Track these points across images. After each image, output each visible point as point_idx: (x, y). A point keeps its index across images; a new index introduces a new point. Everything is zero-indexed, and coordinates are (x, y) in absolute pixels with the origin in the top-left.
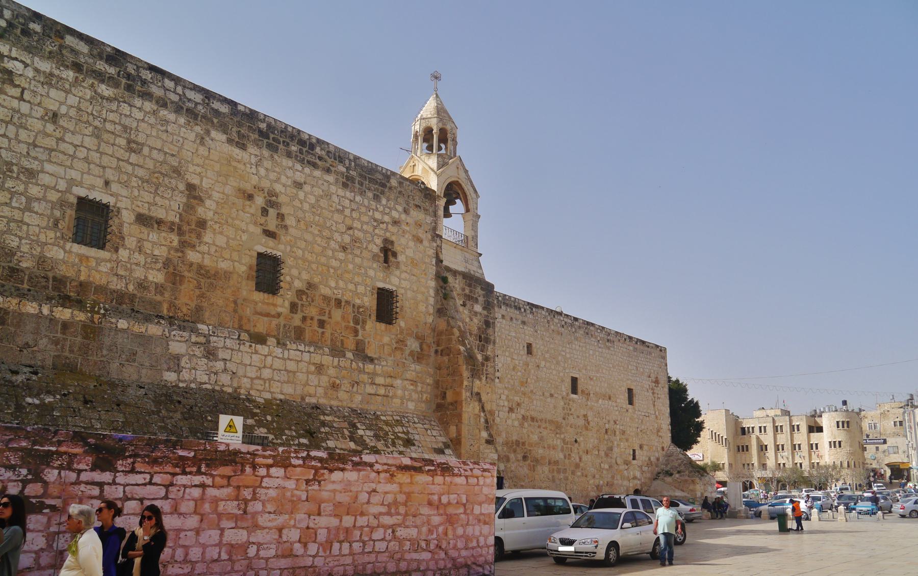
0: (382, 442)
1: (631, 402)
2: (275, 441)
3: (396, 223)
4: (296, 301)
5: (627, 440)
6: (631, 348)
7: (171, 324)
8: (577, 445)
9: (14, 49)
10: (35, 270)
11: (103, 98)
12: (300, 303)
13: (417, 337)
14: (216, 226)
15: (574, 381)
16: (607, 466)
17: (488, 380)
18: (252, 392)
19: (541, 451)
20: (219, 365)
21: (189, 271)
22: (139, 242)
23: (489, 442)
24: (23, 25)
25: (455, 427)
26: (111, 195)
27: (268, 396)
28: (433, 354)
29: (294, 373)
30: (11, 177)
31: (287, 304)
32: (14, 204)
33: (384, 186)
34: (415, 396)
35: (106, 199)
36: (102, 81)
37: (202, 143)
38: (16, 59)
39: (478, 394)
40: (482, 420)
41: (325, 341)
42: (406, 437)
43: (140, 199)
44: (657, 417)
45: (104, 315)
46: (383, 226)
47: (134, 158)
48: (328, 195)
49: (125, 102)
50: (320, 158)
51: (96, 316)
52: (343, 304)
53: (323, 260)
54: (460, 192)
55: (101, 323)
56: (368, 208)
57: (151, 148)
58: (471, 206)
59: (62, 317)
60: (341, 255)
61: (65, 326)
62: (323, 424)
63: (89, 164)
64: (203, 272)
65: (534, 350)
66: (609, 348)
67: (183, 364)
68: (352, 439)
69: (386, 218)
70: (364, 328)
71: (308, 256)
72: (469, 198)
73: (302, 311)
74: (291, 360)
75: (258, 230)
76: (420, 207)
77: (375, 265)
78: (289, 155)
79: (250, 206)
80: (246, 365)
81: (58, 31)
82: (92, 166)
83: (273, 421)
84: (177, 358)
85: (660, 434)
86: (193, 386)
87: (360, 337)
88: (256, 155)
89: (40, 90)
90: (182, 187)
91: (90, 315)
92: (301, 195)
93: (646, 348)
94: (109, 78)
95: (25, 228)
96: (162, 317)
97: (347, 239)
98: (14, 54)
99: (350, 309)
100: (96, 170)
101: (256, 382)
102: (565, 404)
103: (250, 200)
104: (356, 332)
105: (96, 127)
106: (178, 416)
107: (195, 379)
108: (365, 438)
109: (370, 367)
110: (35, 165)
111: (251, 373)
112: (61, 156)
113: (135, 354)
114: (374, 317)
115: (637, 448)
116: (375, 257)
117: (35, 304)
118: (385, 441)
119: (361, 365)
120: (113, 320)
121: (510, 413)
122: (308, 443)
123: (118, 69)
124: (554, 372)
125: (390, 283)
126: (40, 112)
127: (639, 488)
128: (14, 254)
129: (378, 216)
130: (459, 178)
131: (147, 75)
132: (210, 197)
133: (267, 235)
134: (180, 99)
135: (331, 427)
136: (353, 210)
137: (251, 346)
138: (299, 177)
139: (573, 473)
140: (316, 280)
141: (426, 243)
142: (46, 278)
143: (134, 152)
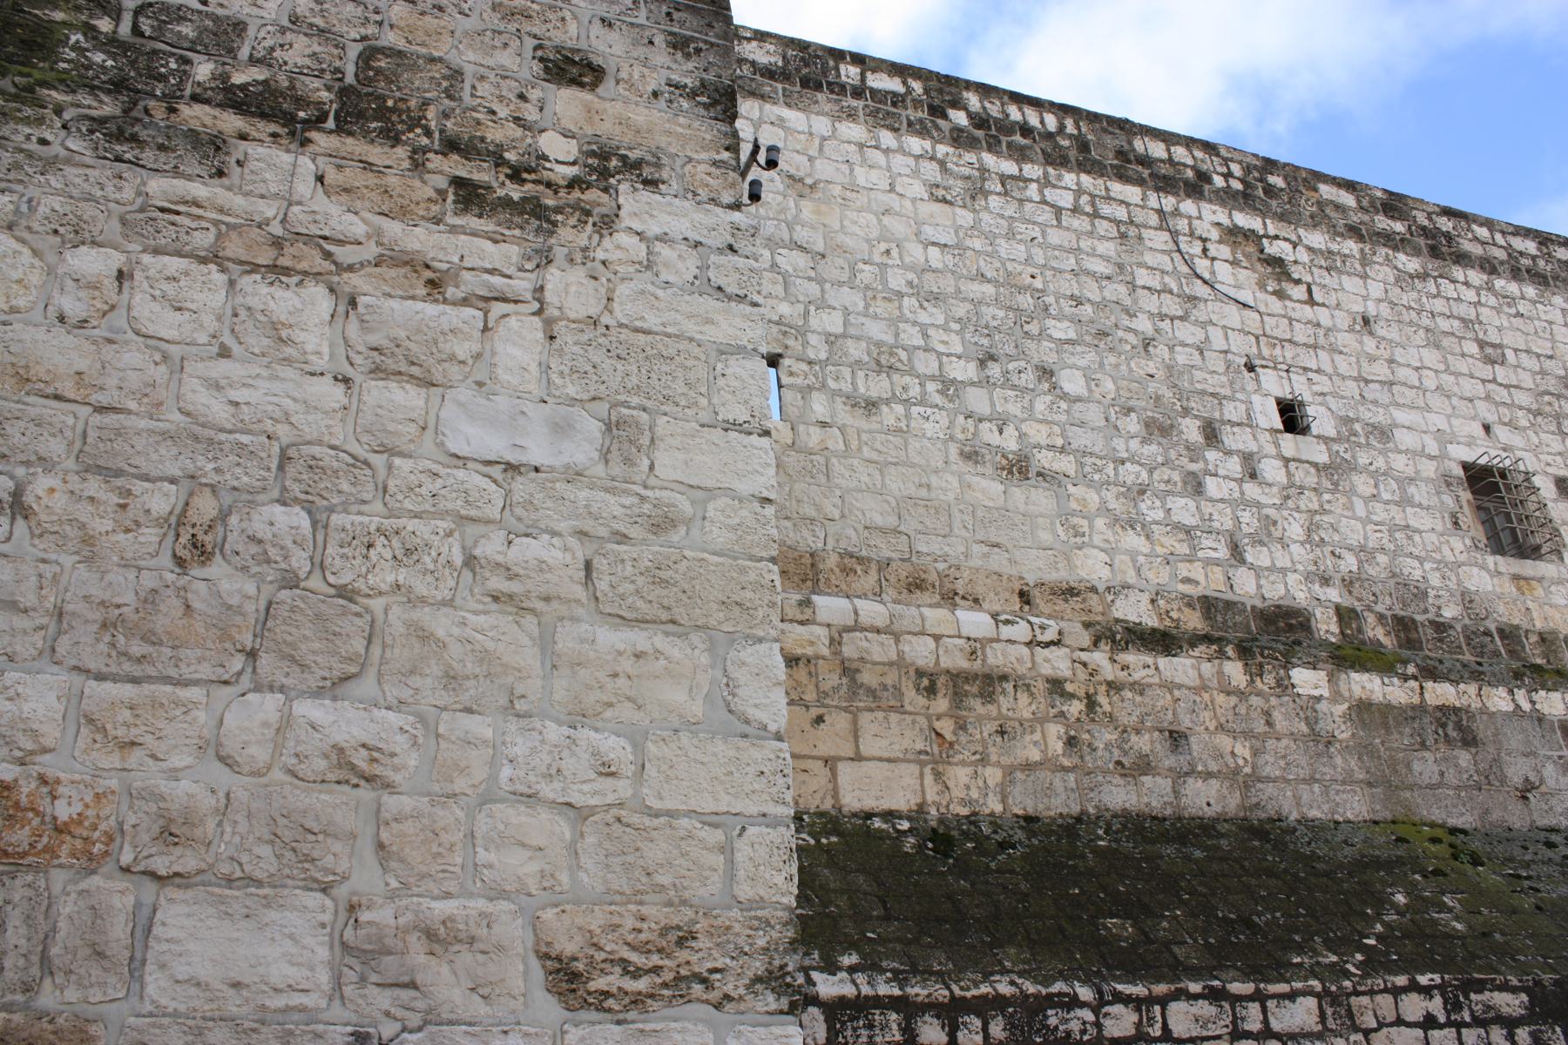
9: (1268, 221)
10: (1467, 621)
24: (1261, 180)
30: (1359, 445)
32: (1386, 496)
36: (1395, 248)
38: (1276, 237)
43: (1546, 449)
47: (1501, 373)
63: (1448, 397)
81: (1305, 180)
89: (1327, 280)
94: (1402, 240)
95: (1417, 538)
98: (1272, 231)
100: (1464, 408)
110: (1380, 417)
112: (1407, 391)
126: (1343, 320)
128: (1425, 594)
131: (1446, 224)
142: (1487, 633)
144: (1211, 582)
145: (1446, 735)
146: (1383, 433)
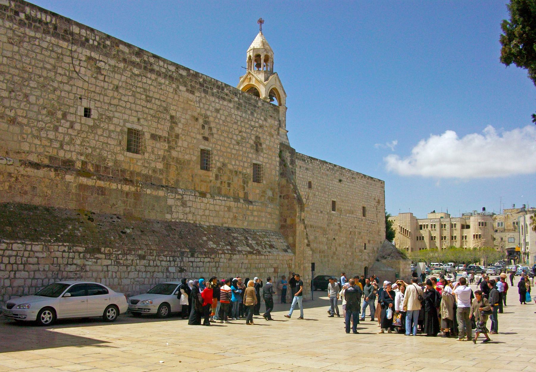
0: (260, 247)
1: (364, 215)
2: (217, 248)
3: (261, 127)
4: (218, 173)
5: (362, 238)
6: (365, 182)
7: (167, 190)
8: (334, 241)
9: (101, 56)
10: (114, 167)
11: (136, 75)
12: (219, 174)
13: (271, 189)
14: (183, 137)
15: (334, 203)
16: (350, 254)
18: (202, 223)
19: (315, 245)
20: (188, 210)
21: (173, 162)
22: (152, 148)
23: (308, 245)
24: (103, 42)
25: (292, 238)
26: (141, 125)
27: (208, 224)
28: (278, 198)
30: (102, 121)
31: (214, 176)
32: (105, 135)
33: (255, 106)
34: (271, 221)
35: (140, 128)
36: (134, 67)
37: (176, 94)
38: (101, 61)
39: (303, 220)
40: (305, 234)
42: (269, 243)
44: (378, 223)
45: (141, 187)
46: (255, 129)
48: (230, 115)
49: (144, 76)
50: (227, 95)
51: (139, 188)
52: (238, 173)
53: (229, 150)
54: (276, 93)
56: (249, 120)
57: (156, 99)
58: (282, 102)
60: (237, 147)
61: (127, 194)
62: (234, 238)
64: (178, 161)
65: (313, 185)
66: (352, 182)
67: (173, 210)
68: (248, 246)
69: (257, 125)
71: (222, 148)
72: (281, 97)
73: (220, 179)
75: (200, 137)
77: (252, 151)
78: (213, 95)
79: (197, 125)
80: (198, 209)
81: (116, 43)
82: (133, 111)
83: (214, 238)
84: (171, 207)
85: (380, 234)
86: (178, 221)
87: (246, 191)
88: (199, 97)
89: (111, 75)
90: (168, 117)
92: (219, 116)
93: (373, 182)
94: (138, 64)
95: (109, 146)
96: (163, 186)
97: (239, 138)
98: (101, 59)
99: (241, 176)
100: (134, 114)
101: (203, 217)
103: (196, 121)
104: (244, 188)
105: (133, 91)
106: (177, 236)
107: (178, 217)
108: (253, 245)
109: (251, 207)
110: (111, 115)
111: (201, 212)
113: (154, 206)
114: (252, 180)
115: (367, 242)
116: (252, 146)
117: (115, 184)
118: (261, 246)
119: (247, 206)
120: (145, 190)
123: (140, 59)
124: (323, 198)
126: (111, 87)
127: (367, 266)
128: (106, 160)
129: (253, 123)
131: (152, 60)
132: (180, 122)
133: (205, 140)
134: (166, 71)
135: (238, 239)
136: (242, 122)
138: (218, 106)
139: (332, 257)
140: (226, 161)
141: (275, 137)
142: (118, 170)
143: (149, 102)
144: (52, 152)
145: (98, 192)
146: (110, 119)
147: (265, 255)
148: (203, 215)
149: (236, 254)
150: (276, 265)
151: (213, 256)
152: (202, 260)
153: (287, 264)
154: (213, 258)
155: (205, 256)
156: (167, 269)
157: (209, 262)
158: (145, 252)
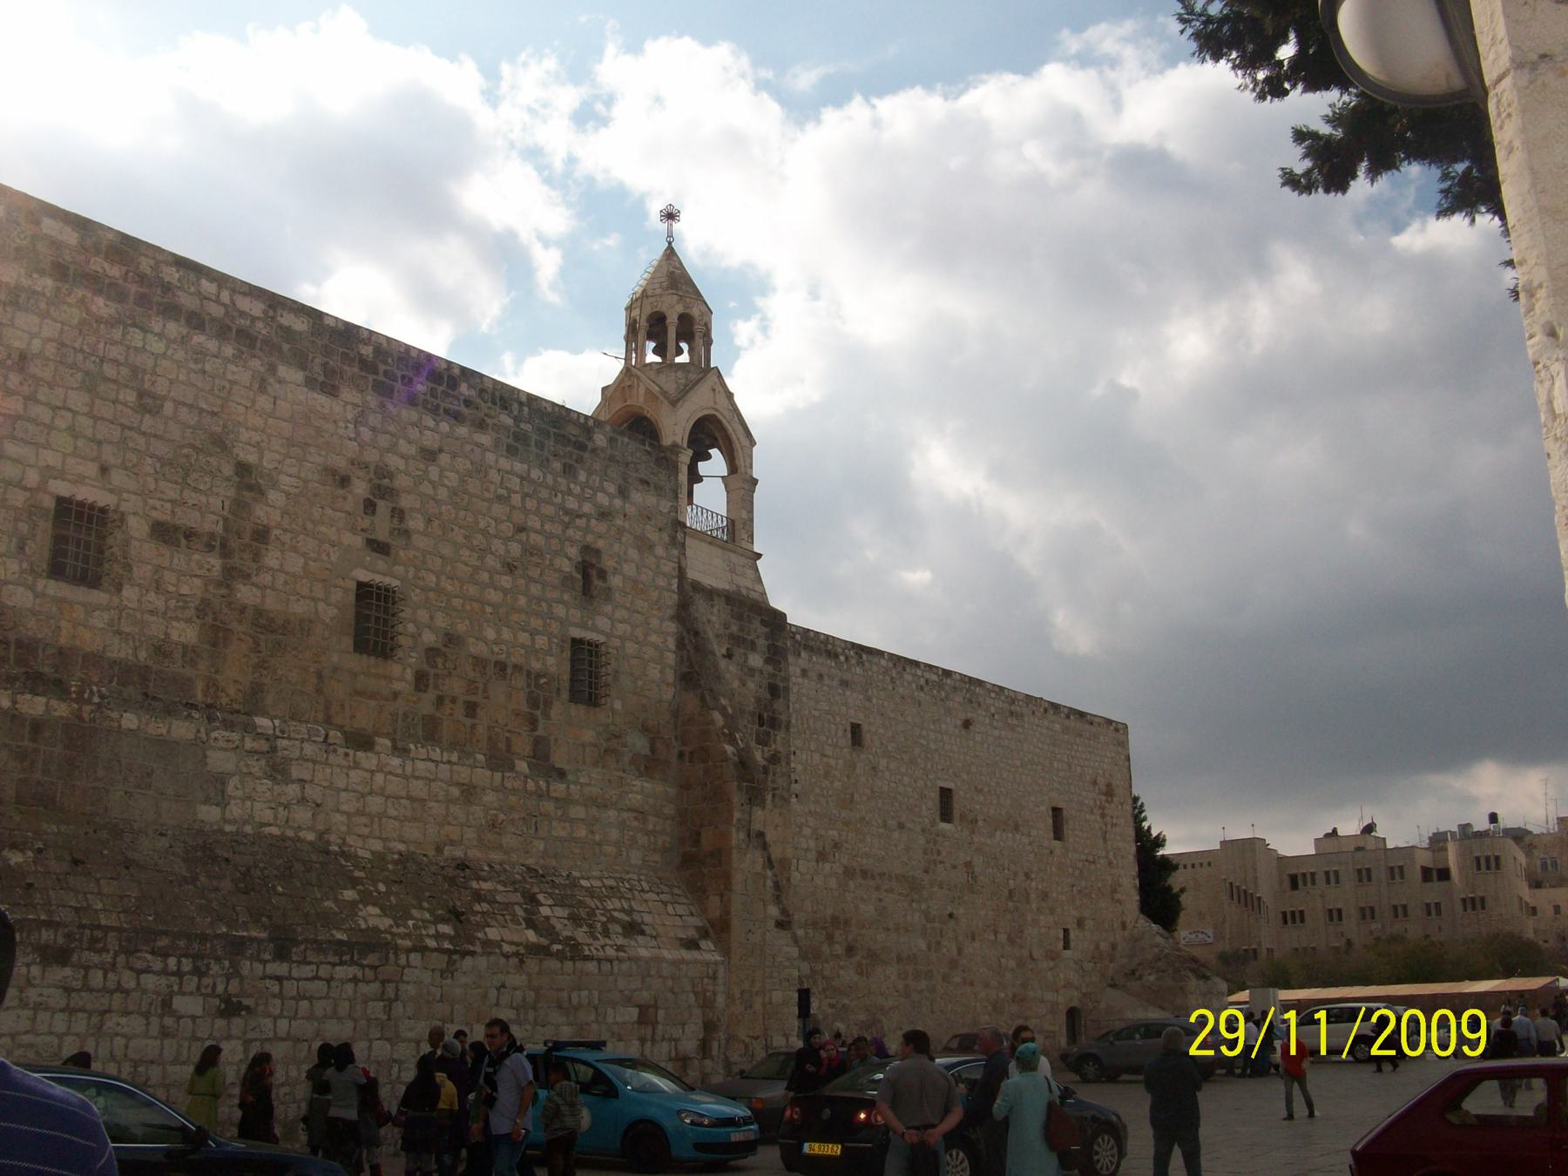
0: (585, 929)
1: (1058, 834)
2: (395, 930)
3: (604, 514)
4: (426, 667)
5: (1052, 911)
6: (1057, 727)
7: (210, 719)
8: (952, 923)
11: (99, 320)
12: (432, 671)
13: (645, 729)
14: (287, 537)
15: (946, 795)
16: (1012, 964)
17: (776, 800)
18: (350, 840)
20: (293, 790)
21: (240, 622)
22: (156, 572)
23: (782, 925)
25: (717, 899)
26: (111, 491)
27: (377, 846)
28: (674, 759)
29: (423, 801)
31: (409, 675)
33: (581, 447)
34: (642, 840)
35: (102, 498)
36: (99, 292)
37: (263, 389)
39: (761, 835)
40: (769, 883)
41: (478, 741)
42: (627, 918)
43: (159, 495)
44: (1110, 863)
45: (99, 706)
46: (581, 522)
47: (148, 420)
48: (480, 470)
49: (135, 325)
50: (468, 403)
51: (87, 708)
52: (509, 671)
53: (472, 590)
55: (95, 721)
56: (554, 490)
57: (178, 404)
58: (740, 462)
59: (31, 712)
60: (506, 581)
61: (37, 727)
62: (478, 896)
63: (76, 437)
64: (263, 621)
65: (867, 737)
66: (1012, 728)
67: (230, 789)
68: (531, 924)
69: (587, 508)
70: (546, 715)
71: (448, 586)
72: (737, 446)
73: (436, 687)
74: (417, 778)
75: (358, 541)
76: (648, 483)
77: (566, 597)
78: (412, 401)
79: (345, 498)
80: (339, 790)
82: (80, 443)
83: (388, 893)
84: (221, 780)
85: (1117, 896)
86: (248, 829)
87: (540, 732)
88: (355, 405)
90: (228, 470)
91: (75, 706)
92: (434, 472)
93: (1087, 726)
94: (110, 284)
96: (194, 706)
97: (515, 549)
99: (520, 681)
102: (928, 842)
103: (343, 487)
104: (533, 722)
105: (87, 373)
106: (226, 885)
107: (251, 816)
108: (553, 921)
109: (558, 788)
111: (348, 803)
112: (31, 427)
113: (149, 775)
114: (565, 695)
115: (1072, 926)
116: (567, 580)
118: (590, 926)
119: (542, 784)
120: (115, 715)
121: (821, 864)
122: (452, 933)
124: (906, 780)
125: (595, 629)
127: (1075, 1003)
129: (572, 504)
130: (716, 410)
132: (275, 485)
133: (374, 550)
135: (492, 902)
136: (526, 495)
137: (347, 755)
138: (430, 440)
140: (462, 627)
141: (660, 551)
143: (150, 412)
147: (599, 960)
148: (360, 813)
149: (473, 953)
150: (645, 994)
151: (371, 959)
152: (324, 971)
153: (696, 994)
154: (374, 968)
155: (336, 959)
156: (166, 1004)
157: (355, 980)
158: (68, 936)
